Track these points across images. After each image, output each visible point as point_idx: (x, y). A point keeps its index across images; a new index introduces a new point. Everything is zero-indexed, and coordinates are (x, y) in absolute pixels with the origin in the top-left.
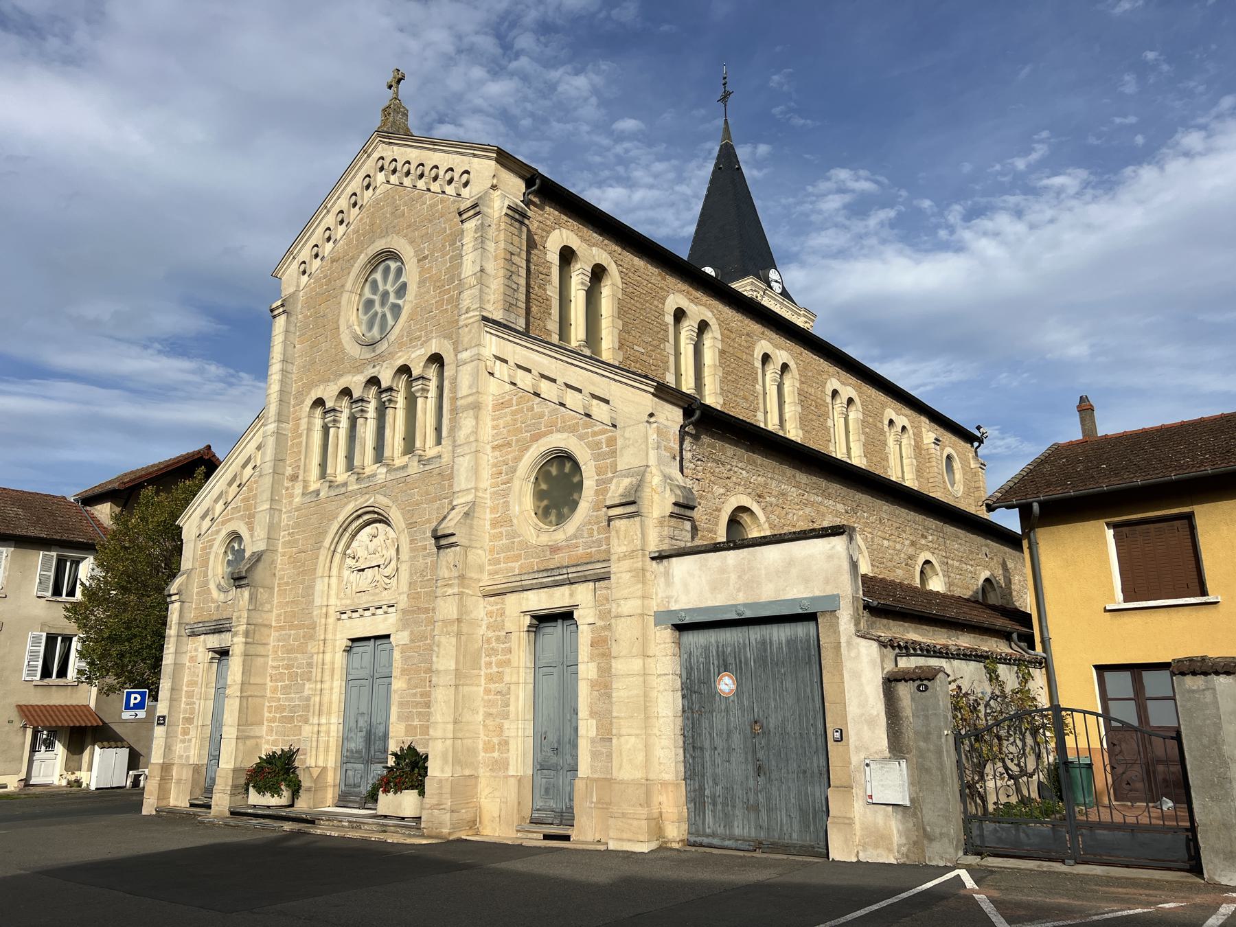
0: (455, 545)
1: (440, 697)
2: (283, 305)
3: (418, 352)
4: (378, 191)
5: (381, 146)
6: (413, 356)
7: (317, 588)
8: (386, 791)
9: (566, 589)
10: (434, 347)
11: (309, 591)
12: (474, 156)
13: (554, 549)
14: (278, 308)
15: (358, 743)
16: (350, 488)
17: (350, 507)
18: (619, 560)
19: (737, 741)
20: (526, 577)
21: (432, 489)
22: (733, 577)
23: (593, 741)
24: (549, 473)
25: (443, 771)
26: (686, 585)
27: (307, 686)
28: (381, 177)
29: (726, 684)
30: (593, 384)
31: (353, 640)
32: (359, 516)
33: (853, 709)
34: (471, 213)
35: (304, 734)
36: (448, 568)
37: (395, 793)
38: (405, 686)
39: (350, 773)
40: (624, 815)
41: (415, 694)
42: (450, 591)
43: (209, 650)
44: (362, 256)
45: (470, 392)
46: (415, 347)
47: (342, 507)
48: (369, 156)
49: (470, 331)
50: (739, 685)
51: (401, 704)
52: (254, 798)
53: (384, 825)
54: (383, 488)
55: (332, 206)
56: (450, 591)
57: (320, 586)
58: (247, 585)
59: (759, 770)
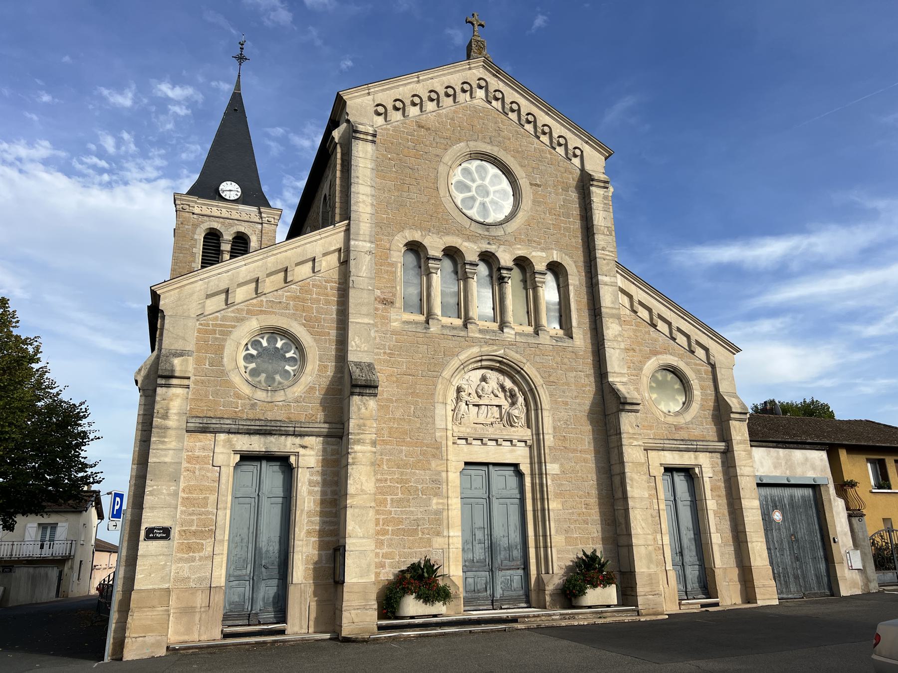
0: (637, 411)
1: (638, 517)
2: (374, 135)
3: (539, 254)
4: (475, 101)
5: (481, 70)
6: (534, 254)
7: (437, 411)
8: (594, 586)
9: (692, 454)
10: (556, 256)
11: (427, 414)
12: (587, 143)
13: (678, 428)
14: (367, 134)
15: (480, 553)
16: (471, 335)
17: (475, 350)
18: (738, 444)
19: (786, 545)
20: (667, 442)
21: (566, 360)
22: (783, 463)
23: (720, 546)
24: (656, 377)
25: (649, 568)
26: (761, 463)
27: (435, 501)
28: (480, 93)
29: (777, 516)
30: (697, 334)
31: (466, 464)
32: (481, 361)
33: (838, 529)
34: (602, 184)
35: (436, 545)
36: (632, 427)
37: (605, 586)
38: (560, 506)
39: (470, 581)
40: (764, 586)
41: (573, 513)
42: (635, 443)
43: (236, 452)
44: (462, 144)
45: (612, 306)
46: (535, 248)
47: (463, 349)
48: (470, 69)
49: (608, 264)
50: (783, 516)
51: (558, 521)
52: (412, 606)
53: (602, 612)
54: (511, 344)
55: (423, 80)
56: (635, 443)
57: (439, 410)
58: (375, 395)
59: (797, 559)
